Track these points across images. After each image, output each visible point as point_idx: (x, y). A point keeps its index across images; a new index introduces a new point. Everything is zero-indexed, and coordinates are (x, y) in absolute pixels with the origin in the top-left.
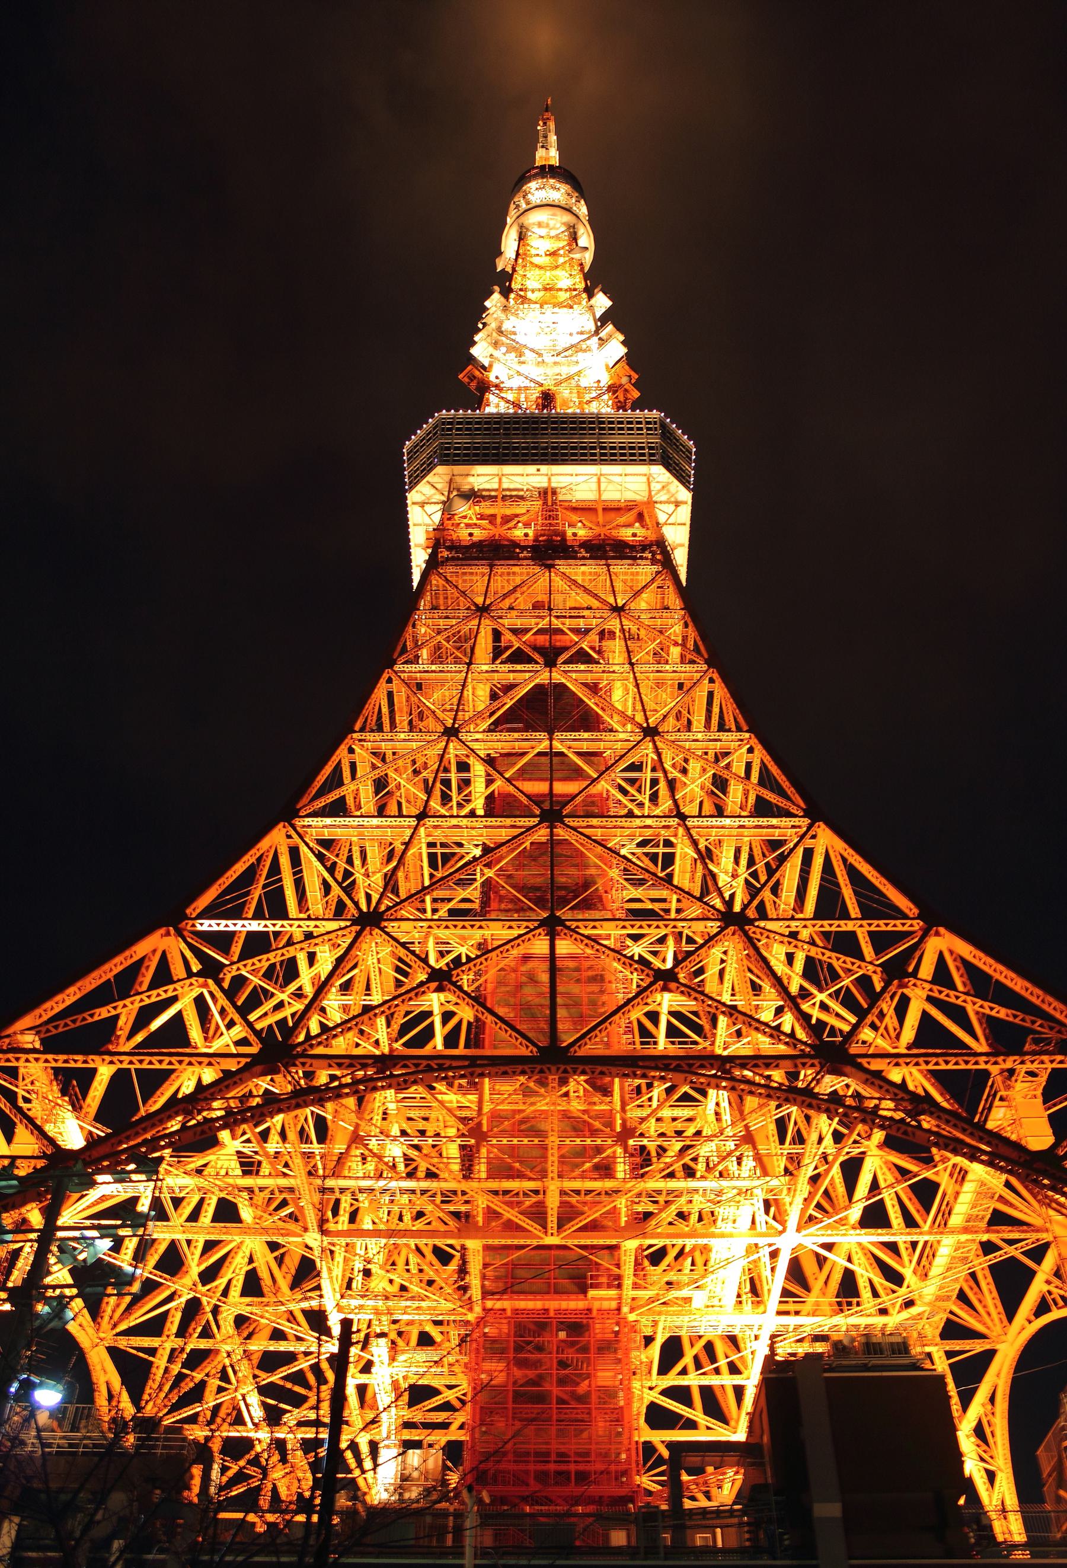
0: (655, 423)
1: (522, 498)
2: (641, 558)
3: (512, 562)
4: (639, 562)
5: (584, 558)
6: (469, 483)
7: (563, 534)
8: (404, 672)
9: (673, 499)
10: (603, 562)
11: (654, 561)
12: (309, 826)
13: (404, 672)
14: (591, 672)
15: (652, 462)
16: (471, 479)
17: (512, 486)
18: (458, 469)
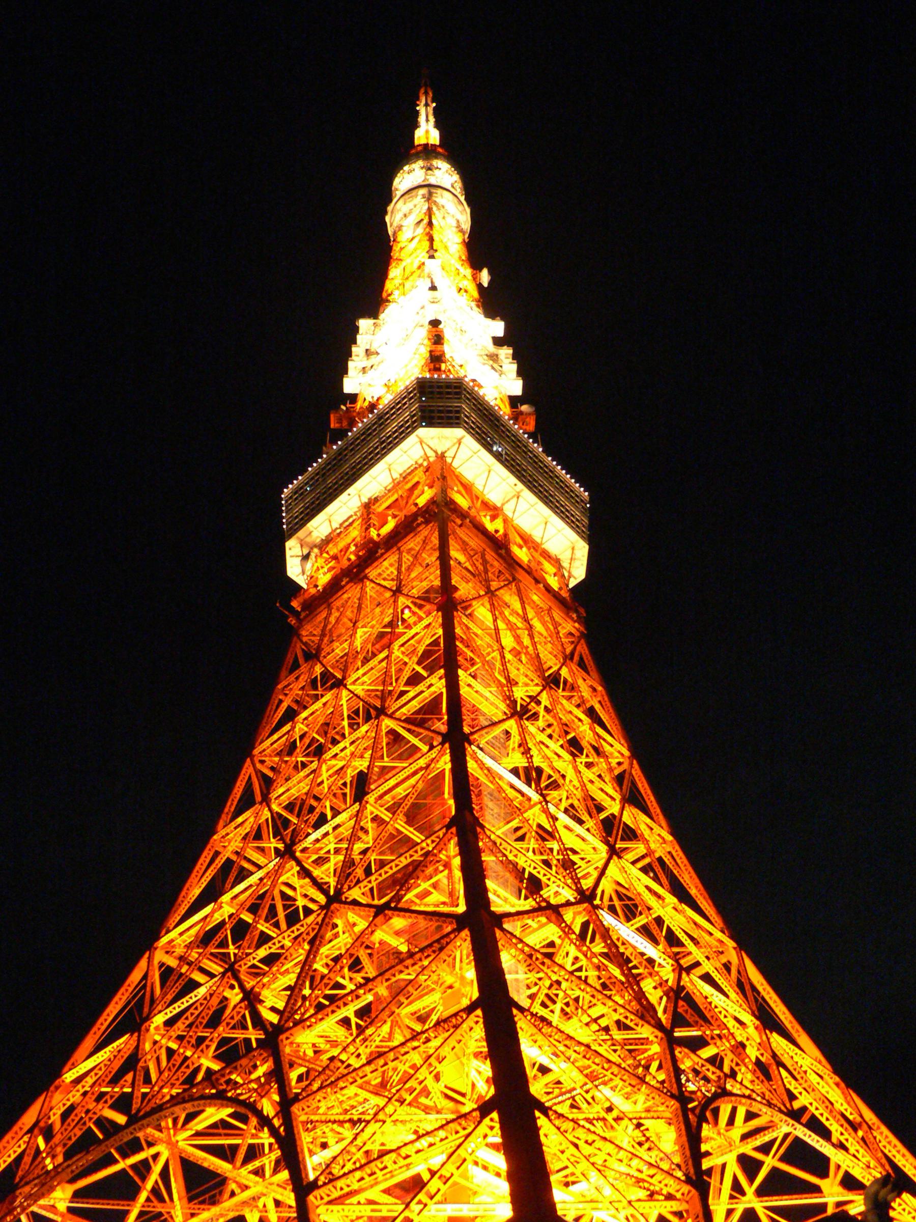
0: (414, 389)
1: (351, 524)
2: (418, 525)
3: (340, 593)
4: (419, 529)
5: (382, 555)
6: (318, 537)
7: (372, 540)
8: (264, 750)
9: (455, 441)
10: (395, 549)
11: (427, 522)
12: (172, 941)
13: (264, 750)
14: (372, 668)
15: (414, 429)
16: (315, 534)
17: (345, 518)
18: (301, 534)
